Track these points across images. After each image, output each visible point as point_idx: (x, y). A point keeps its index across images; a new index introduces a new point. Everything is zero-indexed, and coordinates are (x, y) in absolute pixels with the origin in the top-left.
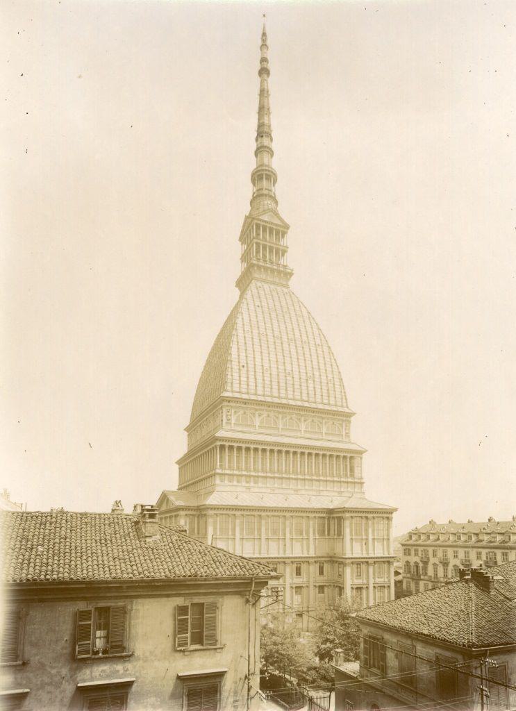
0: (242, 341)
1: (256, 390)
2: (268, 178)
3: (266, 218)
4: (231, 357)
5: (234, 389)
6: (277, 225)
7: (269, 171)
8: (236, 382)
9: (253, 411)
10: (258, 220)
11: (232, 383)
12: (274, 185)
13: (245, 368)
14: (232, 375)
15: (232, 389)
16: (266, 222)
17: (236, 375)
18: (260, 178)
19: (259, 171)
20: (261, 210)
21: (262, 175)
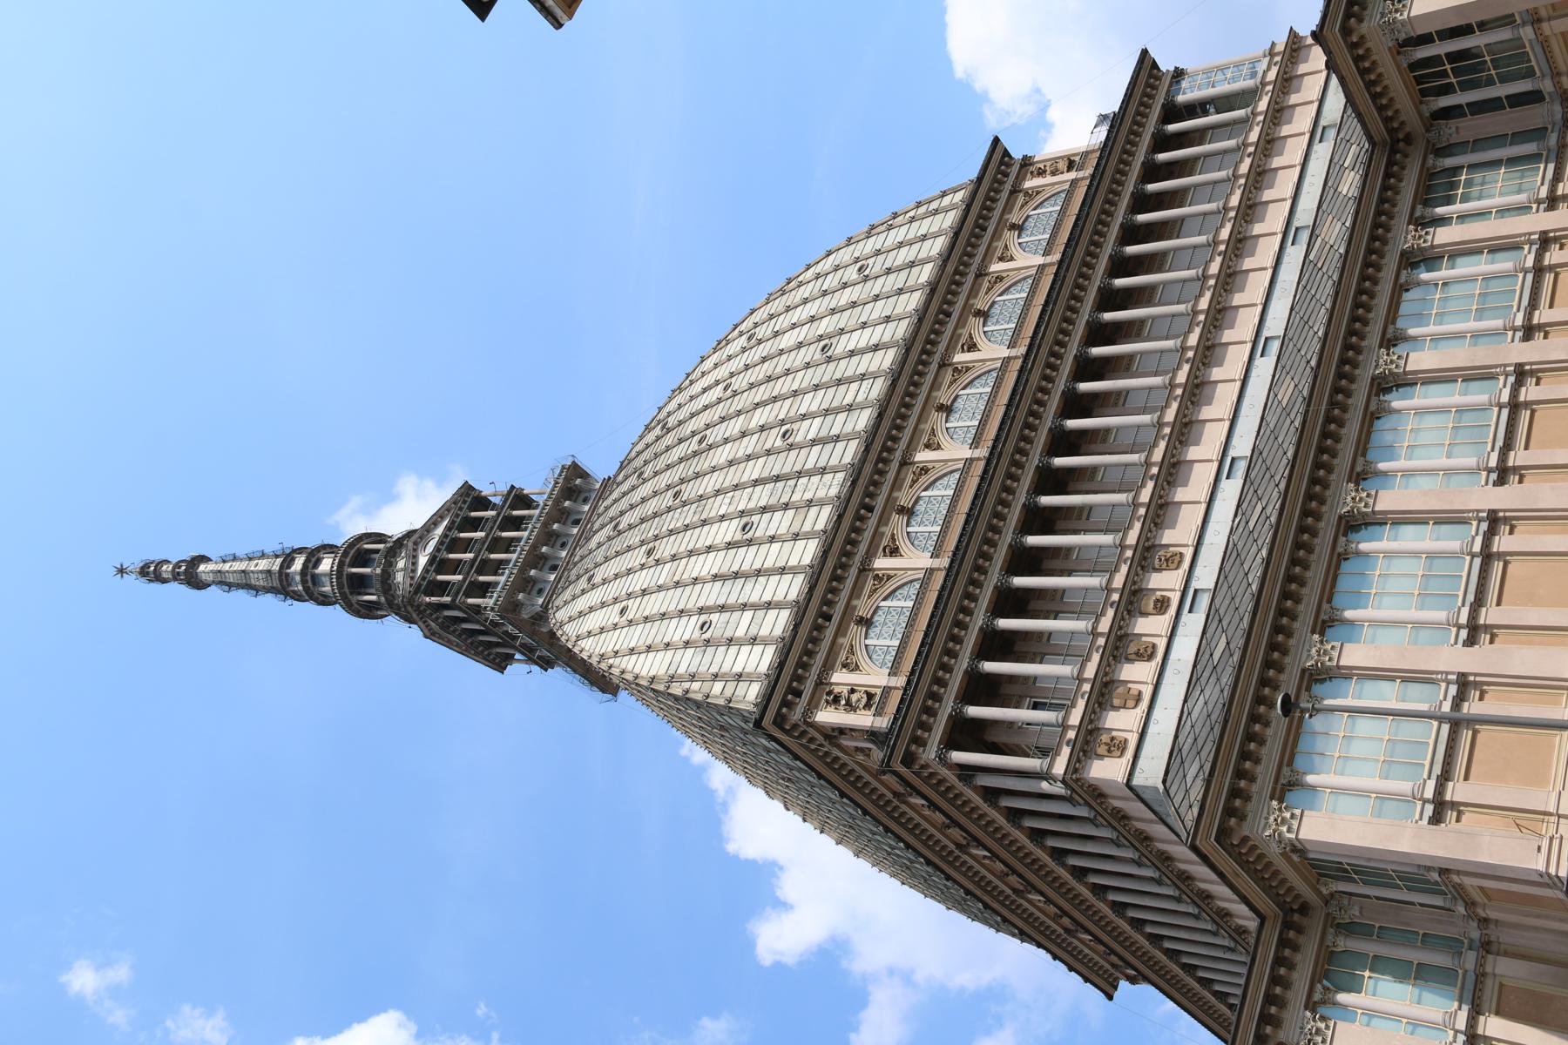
3: (423, 560)
6: (449, 528)
7: (345, 554)
9: (870, 583)
11: (739, 677)
13: (714, 617)
18: (360, 583)
19: (340, 586)
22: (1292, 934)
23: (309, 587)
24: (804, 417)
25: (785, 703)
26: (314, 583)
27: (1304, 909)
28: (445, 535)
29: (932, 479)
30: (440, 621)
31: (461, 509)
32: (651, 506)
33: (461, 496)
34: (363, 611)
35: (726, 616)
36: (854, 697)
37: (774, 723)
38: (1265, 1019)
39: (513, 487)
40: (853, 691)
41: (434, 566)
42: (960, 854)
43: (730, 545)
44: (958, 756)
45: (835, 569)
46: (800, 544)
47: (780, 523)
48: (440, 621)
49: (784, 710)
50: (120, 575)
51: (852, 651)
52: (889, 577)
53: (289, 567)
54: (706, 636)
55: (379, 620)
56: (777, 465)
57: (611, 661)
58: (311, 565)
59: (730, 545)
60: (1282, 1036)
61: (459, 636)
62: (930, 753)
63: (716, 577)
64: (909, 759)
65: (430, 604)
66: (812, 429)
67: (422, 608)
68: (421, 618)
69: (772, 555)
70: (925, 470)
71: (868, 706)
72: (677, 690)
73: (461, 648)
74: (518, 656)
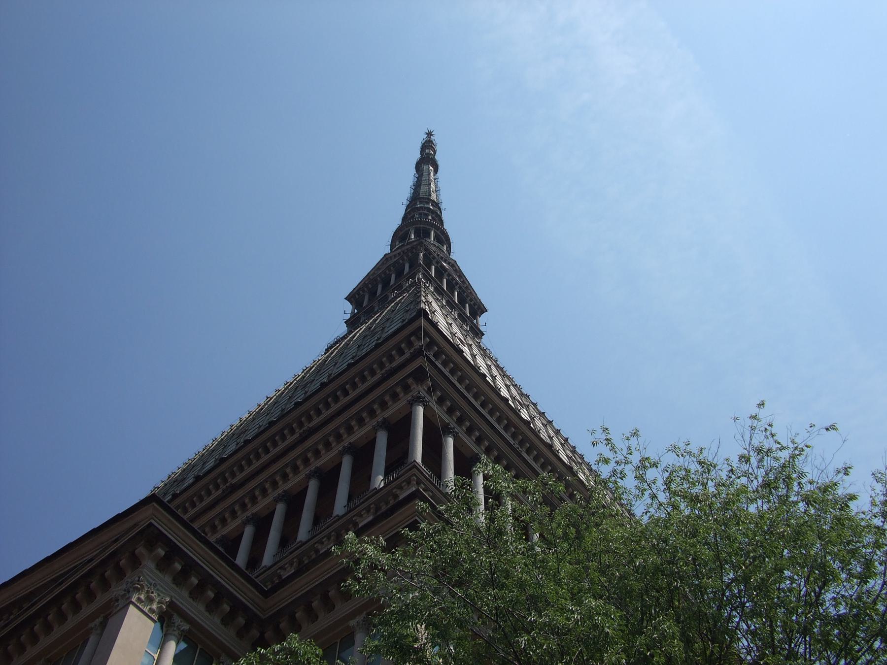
22: (241, 621)
28: (457, 283)
30: (401, 261)
34: (401, 234)
38: (174, 551)
39: (483, 334)
42: (228, 484)
45: (516, 427)
48: (401, 261)
50: (427, 132)
55: (390, 244)
58: (434, 216)
60: (149, 565)
61: (384, 272)
65: (418, 255)
67: (414, 250)
68: (403, 252)
73: (372, 275)
74: (356, 311)
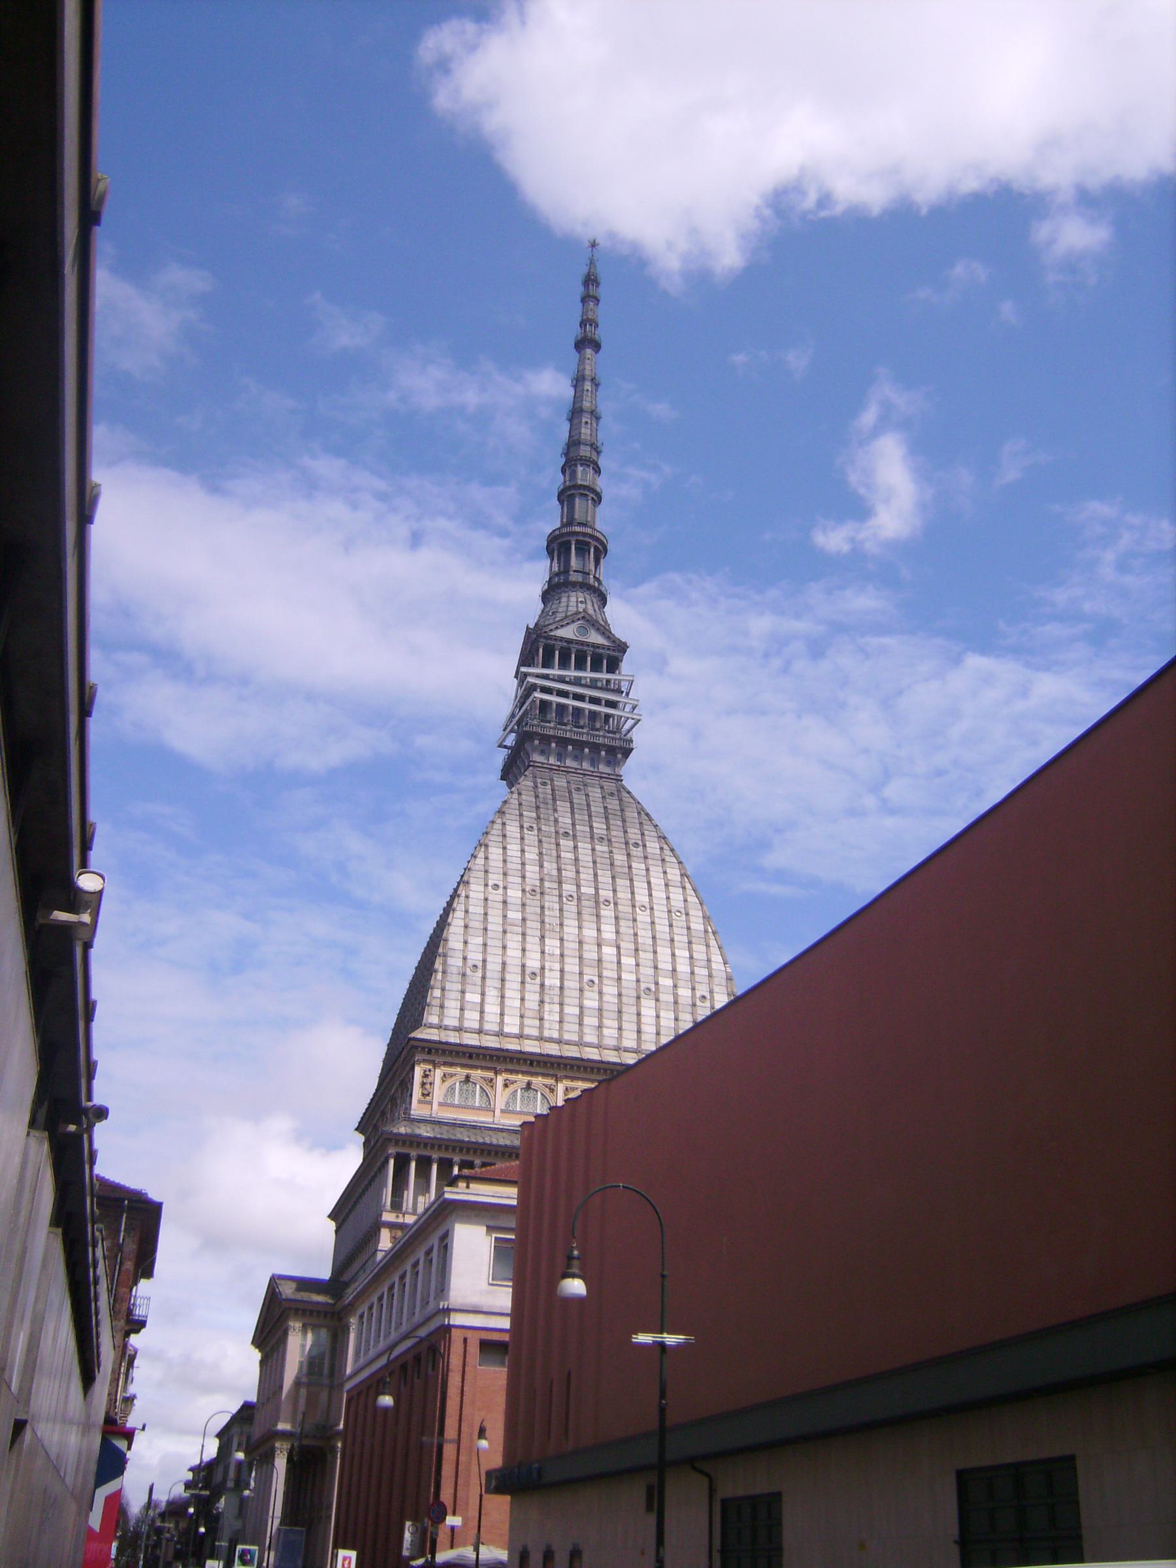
0: (476, 909)
1: (502, 1023)
2: (583, 549)
3: (568, 632)
4: (444, 946)
5: (448, 1022)
7: (585, 534)
8: (452, 1006)
10: (550, 637)
11: (442, 1007)
12: (597, 562)
13: (479, 974)
14: (443, 989)
15: (441, 1020)
16: (569, 641)
17: (453, 986)
19: (562, 535)
20: (560, 616)
21: (569, 543)
23: (566, 492)
24: (600, 993)
25: (423, 1048)
26: (569, 496)
27: (340, 1319)
29: (547, 1096)
31: (609, 649)
32: (569, 873)
33: (619, 645)
35: (479, 981)
36: (428, 1086)
37: (413, 1047)
40: (431, 1084)
41: (565, 644)
43: (523, 966)
44: (392, 1162)
46: (517, 1021)
47: (532, 998)
49: (420, 1049)
51: (452, 1075)
52: (492, 1087)
53: (582, 465)
54: (469, 972)
56: (572, 984)
57: (463, 894)
59: (523, 966)
62: (392, 1150)
63: (504, 964)
64: (390, 1140)
66: (591, 1002)
69: (513, 1002)
70: (552, 1090)
71: (423, 1095)
72: (438, 965)
